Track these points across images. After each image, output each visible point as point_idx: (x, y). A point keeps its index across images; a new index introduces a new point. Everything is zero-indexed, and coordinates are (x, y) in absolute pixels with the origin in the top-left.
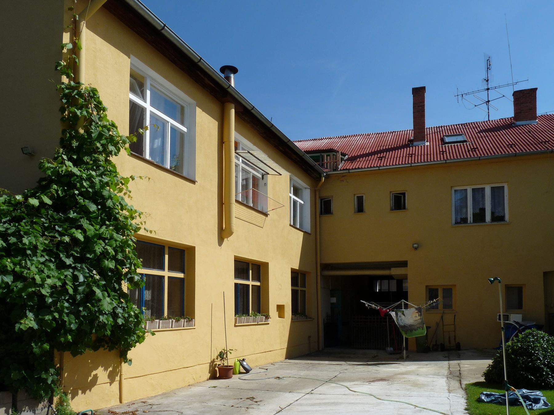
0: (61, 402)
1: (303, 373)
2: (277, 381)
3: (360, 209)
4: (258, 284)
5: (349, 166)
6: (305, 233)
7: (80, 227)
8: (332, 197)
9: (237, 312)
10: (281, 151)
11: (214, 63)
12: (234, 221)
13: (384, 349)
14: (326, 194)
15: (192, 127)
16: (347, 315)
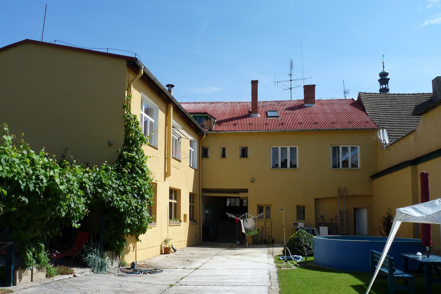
0: (123, 257)
1: (202, 252)
2: (192, 255)
3: (224, 156)
4: (176, 202)
5: (219, 128)
6: (195, 169)
7: (137, 181)
8: (209, 147)
9: (171, 218)
10: (187, 123)
11: (163, 82)
12: (172, 168)
13: (235, 243)
14: (205, 145)
15: (156, 119)
16: (218, 222)
